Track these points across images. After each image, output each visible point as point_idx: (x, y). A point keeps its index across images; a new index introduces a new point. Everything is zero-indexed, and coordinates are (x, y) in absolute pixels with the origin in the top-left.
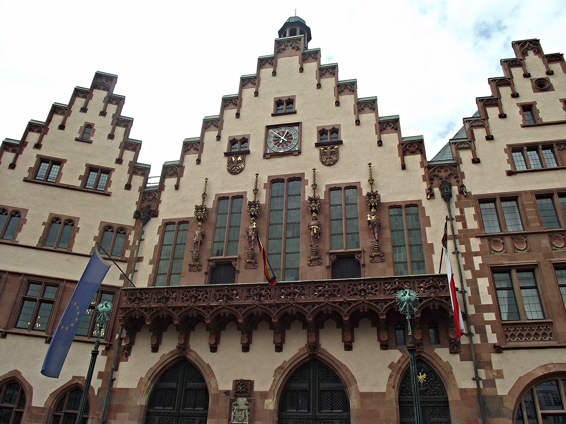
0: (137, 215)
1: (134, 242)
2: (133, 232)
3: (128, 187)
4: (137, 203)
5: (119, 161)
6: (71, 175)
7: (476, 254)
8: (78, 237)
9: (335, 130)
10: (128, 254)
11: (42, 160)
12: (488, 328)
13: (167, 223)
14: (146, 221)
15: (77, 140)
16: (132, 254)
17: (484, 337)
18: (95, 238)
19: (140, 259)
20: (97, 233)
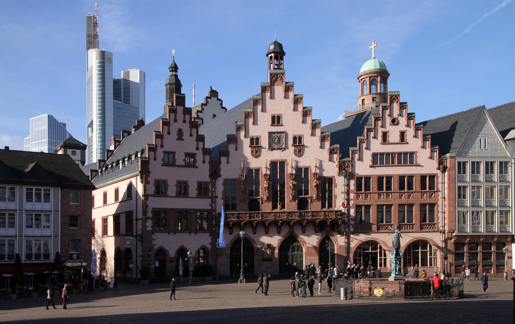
0: (211, 176)
1: (212, 189)
2: (210, 184)
3: (204, 162)
4: (209, 170)
5: (197, 149)
6: (180, 160)
7: (352, 200)
8: (190, 190)
9: (300, 138)
10: (210, 195)
11: (165, 152)
12: (351, 226)
13: (226, 181)
14: (215, 179)
15: (177, 139)
16: (212, 194)
17: (349, 229)
18: (196, 189)
19: (217, 197)
20: (196, 187)
